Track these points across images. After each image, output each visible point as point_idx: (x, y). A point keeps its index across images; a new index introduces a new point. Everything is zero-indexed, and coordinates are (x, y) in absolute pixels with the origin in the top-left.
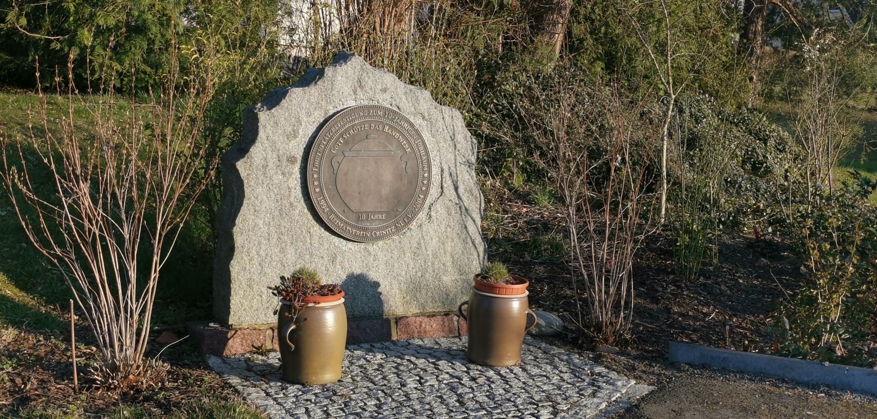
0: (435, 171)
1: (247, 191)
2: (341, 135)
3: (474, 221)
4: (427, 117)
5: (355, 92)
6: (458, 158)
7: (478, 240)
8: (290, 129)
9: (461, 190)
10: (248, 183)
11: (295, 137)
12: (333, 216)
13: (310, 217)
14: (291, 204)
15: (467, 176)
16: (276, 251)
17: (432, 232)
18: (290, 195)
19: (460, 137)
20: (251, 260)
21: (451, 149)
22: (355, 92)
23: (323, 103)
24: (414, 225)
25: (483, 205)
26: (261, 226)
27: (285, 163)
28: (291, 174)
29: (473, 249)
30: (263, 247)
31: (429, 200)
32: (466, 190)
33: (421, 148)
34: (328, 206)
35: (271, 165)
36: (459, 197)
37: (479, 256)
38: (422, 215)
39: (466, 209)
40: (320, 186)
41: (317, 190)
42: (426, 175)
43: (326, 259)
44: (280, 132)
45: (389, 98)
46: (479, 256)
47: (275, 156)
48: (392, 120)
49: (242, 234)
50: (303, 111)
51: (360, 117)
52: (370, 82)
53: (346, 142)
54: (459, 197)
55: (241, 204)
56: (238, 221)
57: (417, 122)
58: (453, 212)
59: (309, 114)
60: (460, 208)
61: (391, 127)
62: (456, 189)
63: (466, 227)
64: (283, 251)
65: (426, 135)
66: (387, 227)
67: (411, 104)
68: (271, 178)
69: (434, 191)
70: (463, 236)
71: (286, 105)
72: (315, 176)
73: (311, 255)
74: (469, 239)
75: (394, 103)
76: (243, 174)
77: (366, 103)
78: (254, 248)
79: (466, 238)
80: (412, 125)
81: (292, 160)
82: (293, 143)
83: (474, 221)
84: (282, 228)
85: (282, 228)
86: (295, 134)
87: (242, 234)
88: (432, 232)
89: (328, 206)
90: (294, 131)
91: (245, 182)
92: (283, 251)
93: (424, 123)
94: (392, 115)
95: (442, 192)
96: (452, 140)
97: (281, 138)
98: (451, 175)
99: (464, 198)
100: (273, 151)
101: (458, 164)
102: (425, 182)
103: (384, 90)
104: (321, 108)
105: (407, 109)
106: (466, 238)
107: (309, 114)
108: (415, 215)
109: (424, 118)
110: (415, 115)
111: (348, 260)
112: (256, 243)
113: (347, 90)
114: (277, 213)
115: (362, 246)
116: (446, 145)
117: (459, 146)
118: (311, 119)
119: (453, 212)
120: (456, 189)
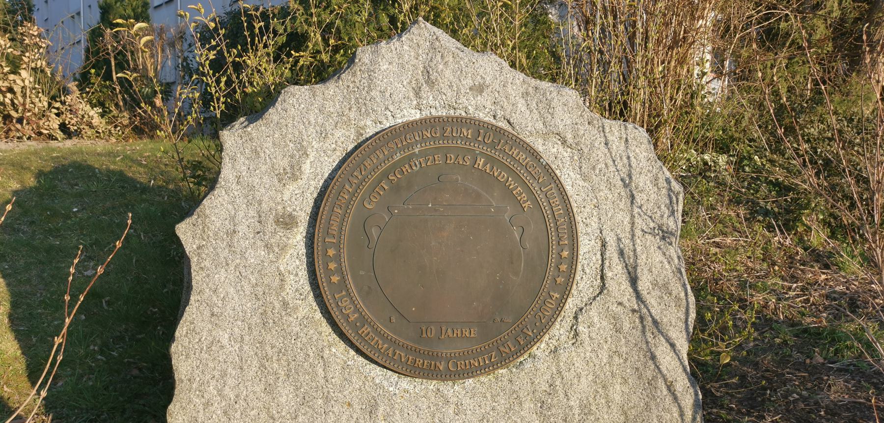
0: (587, 246)
1: (197, 278)
2: (385, 175)
3: (673, 345)
4: (570, 140)
5: (417, 93)
6: (638, 221)
7: (682, 383)
8: (283, 163)
9: (644, 284)
10: (199, 263)
11: (294, 178)
12: (366, 329)
13: (326, 328)
14: (285, 304)
15: (658, 257)
16: (258, 389)
17: (579, 363)
18: (282, 287)
19: (642, 181)
20: (207, 404)
21: (624, 204)
22: (417, 93)
23: (352, 115)
24: (540, 349)
25: (693, 315)
26: (225, 341)
27: (270, 226)
28: (284, 248)
29: (669, 400)
30: (231, 382)
31: (571, 305)
32: (655, 284)
33: (557, 200)
34: (357, 310)
35: (242, 229)
36: (638, 296)
37: (682, 415)
38: (560, 330)
39: (655, 322)
40: (339, 271)
41: (335, 279)
42: (565, 254)
43: (356, 406)
44: (264, 168)
45: (489, 105)
46: (682, 415)
47: (252, 213)
48: (493, 146)
49: (187, 356)
50: (311, 129)
51: (424, 140)
52: (448, 73)
53: (396, 188)
54: (638, 296)
55: (187, 302)
56: (181, 331)
57: (550, 151)
58: (627, 326)
59: (323, 135)
60: (642, 319)
61: (490, 159)
62: (634, 281)
63: (653, 358)
64: (269, 389)
65: (570, 179)
66: (482, 353)
67: (536, 116)
68: (243, 255)
69: (584, 284)
70: (649, 374)
71: (275, 118)
72: (331, 252)
73: (327, 399)
74: (661, 383)
75: (500, 114)
76: (189, 247)
77: (443, 113)
78: (213, 383)
79: (654, 378)
80: (535, 155)
81: (287, 222)
82: (292, 187)
83: (673, 345)
84: (268, 348)
85: (268, 348)
86: (293, 173)
87: (187, 356)
88: (579, 363)
89: (357, 310)
90: (292, 167)
91: (194, 260)
92: (269, 389)
93: (566, 153)
94: (497, 138)
95: (603, 287)
96: (626, 186)
97: (266, 179)
98: (621, 253)
99: (651, 301)
100: (249, 204)
101: (638, 233)
102: (564, 267)
103: (479, 89)
104: (348, 123)
105: (526, 121)
106: (654, 378)
107: (323, 135)
108: (544, 328)
109: (564, 142)
110: (545, 136)
111: (401, 411)
112: (216, 373)
113: (401, 88)
114: (256, 319)
115: (432, 385)
116: (611, 196)
117: (639, 198)
118: (328, 145)
119: (627, 326)
120: (634, 281)
